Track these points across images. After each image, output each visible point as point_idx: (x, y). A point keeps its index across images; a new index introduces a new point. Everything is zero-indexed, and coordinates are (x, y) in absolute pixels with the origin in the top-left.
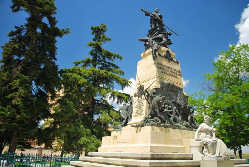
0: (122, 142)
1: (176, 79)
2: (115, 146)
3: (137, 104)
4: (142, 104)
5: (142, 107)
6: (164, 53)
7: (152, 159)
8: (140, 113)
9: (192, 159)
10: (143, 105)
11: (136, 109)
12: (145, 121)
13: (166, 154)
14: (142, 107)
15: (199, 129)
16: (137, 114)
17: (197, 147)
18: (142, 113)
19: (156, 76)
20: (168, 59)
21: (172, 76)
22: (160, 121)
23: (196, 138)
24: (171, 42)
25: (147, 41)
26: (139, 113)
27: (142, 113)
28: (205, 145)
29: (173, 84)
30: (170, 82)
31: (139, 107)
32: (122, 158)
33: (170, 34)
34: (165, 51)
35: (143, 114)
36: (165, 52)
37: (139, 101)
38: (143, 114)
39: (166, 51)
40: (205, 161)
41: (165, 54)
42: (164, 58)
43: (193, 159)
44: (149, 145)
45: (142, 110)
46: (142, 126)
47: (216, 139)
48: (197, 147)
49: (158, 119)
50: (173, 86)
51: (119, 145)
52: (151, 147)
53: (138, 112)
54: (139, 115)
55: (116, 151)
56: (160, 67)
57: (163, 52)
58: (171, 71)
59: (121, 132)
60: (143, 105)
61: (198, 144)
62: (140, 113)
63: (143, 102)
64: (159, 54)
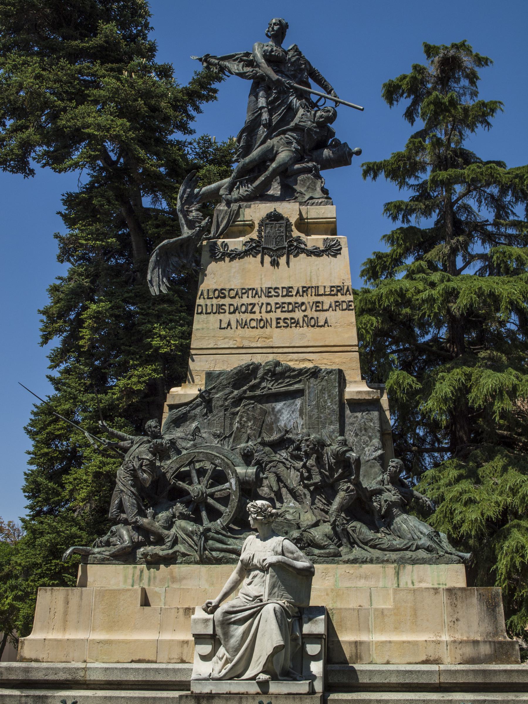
13: (47, 668)
20: (265, 251)
50: (278, 372)
56: (220, 306)
58: (280, 306)
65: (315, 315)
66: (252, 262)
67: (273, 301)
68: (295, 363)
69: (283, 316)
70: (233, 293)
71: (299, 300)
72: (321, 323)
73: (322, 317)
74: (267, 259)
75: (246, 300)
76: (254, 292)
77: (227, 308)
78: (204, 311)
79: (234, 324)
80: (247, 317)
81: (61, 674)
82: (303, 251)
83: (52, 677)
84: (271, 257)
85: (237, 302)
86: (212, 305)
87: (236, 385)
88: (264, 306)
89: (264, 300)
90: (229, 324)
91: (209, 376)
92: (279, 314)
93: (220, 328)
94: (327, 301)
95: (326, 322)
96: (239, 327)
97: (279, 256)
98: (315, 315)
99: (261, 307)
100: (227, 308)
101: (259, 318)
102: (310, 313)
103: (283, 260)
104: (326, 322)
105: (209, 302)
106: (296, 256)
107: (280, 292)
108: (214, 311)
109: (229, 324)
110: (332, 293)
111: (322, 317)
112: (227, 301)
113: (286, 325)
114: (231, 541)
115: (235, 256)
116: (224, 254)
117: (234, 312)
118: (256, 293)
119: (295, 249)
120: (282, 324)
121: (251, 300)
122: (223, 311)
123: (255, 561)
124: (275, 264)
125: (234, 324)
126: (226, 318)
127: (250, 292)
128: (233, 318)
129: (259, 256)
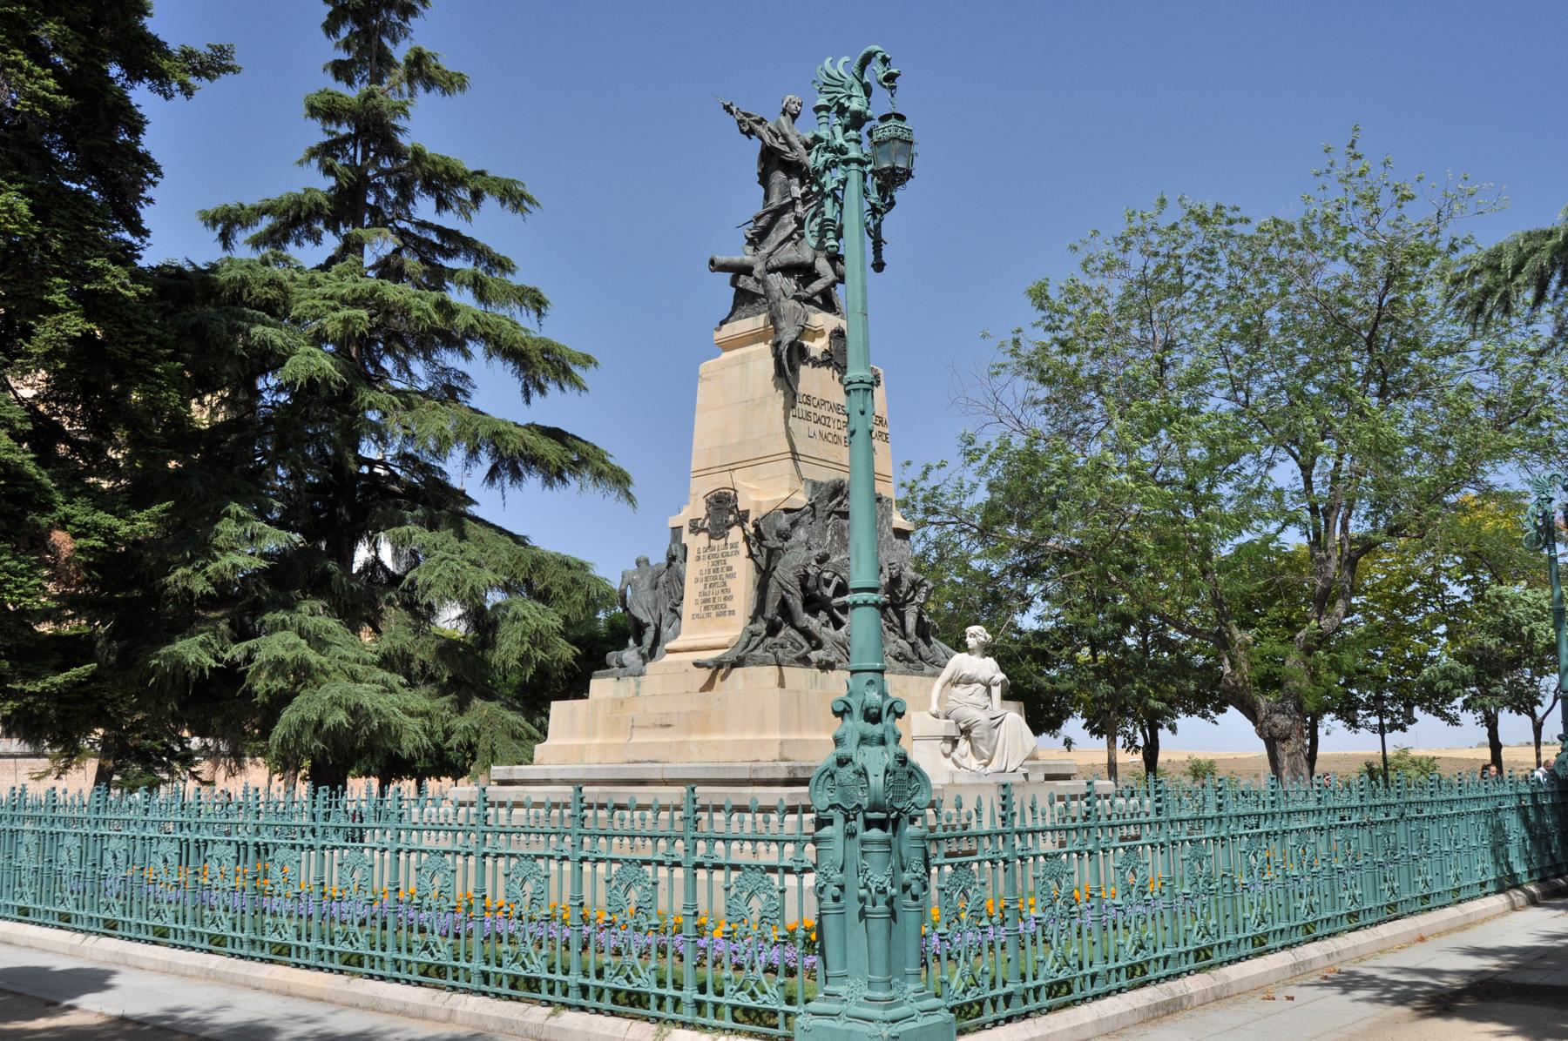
0: (654, 726)
2: (621, 740)
3: (704, 565)
4: (730, 568)
5: (729, 582)
10: (733, 576)
11: (700, 587)
15: (946, 674)
17: (934, 738)
18: (730, 606)
22: (806, 646)
23: (934, 708)
25: (747, 270)
26: (714, 607)
27: (730, 606)
31: (717, 578)
35: (732, 613)
37: (715, 556)
38: (732, 613)
40: (961, 785)
42: (824, 369)
46: (739, 663)
48: (934, 738)
49: (800, 639)
51: (639, 738)
52: (782, 743)
54: (714, 613)
55: (632, 757)
56: (808, 413)
59: (639, 685)
60: (733, 576)
61: (944, 727)
62: (716, 607)
63: (730, 561)
80: (825, 430)
89: (835, 415)
112: (811, 409)
128: (819, 427)
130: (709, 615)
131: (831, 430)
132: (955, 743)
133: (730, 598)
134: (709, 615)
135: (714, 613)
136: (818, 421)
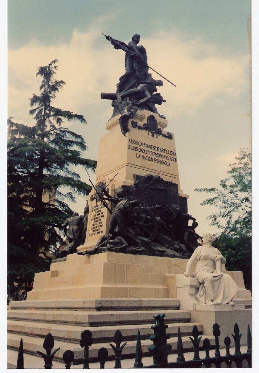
1: (164, 165)
4: (102, 213)
6: (145, 121)
7: (99, 309)
8: (97, 230)
9: (178, 308)
12: (100, 243)
14: (102, 219)
16: (94, 231)
19: (126, 164)
21: (159, 161)
24: (162, 98)
28: (200, 284)
29: (159, 177)
30: (154, 174)
31: (97, 219)
32: (58, 308)
33: (160, 83)
34: (147, 117)
36: (146, 119)
38: (102, 232)
39: (148, 118)
41: (146, 122)
42: (144, 131)
43: (182, 307)
44: (101, 285)
45: (101, 224)
47: (222, 273)
50: (159, 180)
53: (94, 228)
56: (136, 148)
57: (142, 118)
60: (103, 216)
62: (97, 230)
64: (133, 122)
65: (167, 161)
66: (145, 133)
67: (153, 151)
68: (165, 178)
69: (157, 158)
70: (140, 144)
71: (162, 153)
72: (168, 164)
73: (169, 162)
74: (151, 134)
75: (144, 148)
76: (147, 145)
77: (138, 149)
78: (130, 148)
79: (141, 156)
81: (133, 304)
82: (161, 134)
83: (130, 305)
84: (152, 133)
85: (142, 148)
86: (133, 146)
87: (146, 183)
88: (150, 153)
89: (150, 150)
90: (139, 156)
91: (137, 177)
92: (154, 157)
93: (136, 157)
94: (170, 156)
95: (170, 164)
96: (143, 159)
97: (154, 133)
98: (167, 161)
99: (149, 152)
100: (138, 149)
101: (149, 157)
102: (165, 160)
103: (155, 135)
104: (170, 164)
105: (133, 145)
106: (159, 135)
107: (155, 148)
108: (134, 149)
109: (139, 156)
110: (171, 154)
111: (169, 162)
113: (157, 162)
114: (157, 247)
115: (140, 128)
116: (137, 126)
117: (141, 152)
118: (148, 146)
119: (159, 132)
120: (156, 161)
121: (146, 149)
122: (137, 150)
123: (210, 257)
124: (153, 136)
125: (141, 156)
126: (138, 153)
127: (146, 145)
128: (141, 154)
129: (148, 131)
130: (94, 234)
131: (148, 156)
132: (197, 289)
133: (101, 226)
134: (94, 234)
135: (96, 232)
136: (142, 151)
